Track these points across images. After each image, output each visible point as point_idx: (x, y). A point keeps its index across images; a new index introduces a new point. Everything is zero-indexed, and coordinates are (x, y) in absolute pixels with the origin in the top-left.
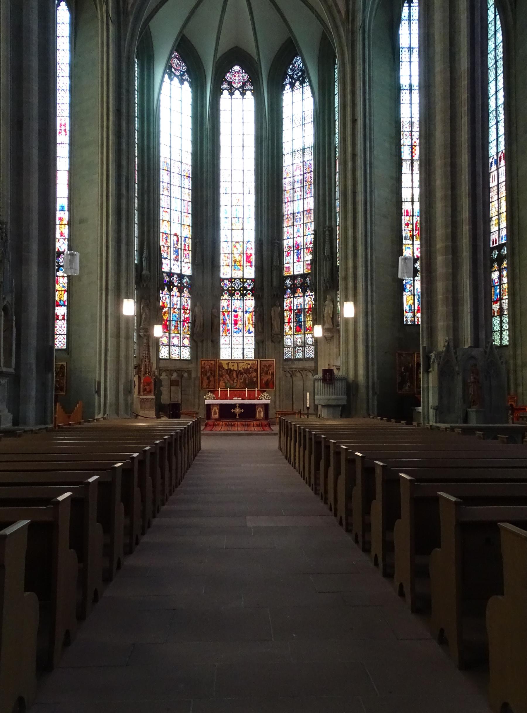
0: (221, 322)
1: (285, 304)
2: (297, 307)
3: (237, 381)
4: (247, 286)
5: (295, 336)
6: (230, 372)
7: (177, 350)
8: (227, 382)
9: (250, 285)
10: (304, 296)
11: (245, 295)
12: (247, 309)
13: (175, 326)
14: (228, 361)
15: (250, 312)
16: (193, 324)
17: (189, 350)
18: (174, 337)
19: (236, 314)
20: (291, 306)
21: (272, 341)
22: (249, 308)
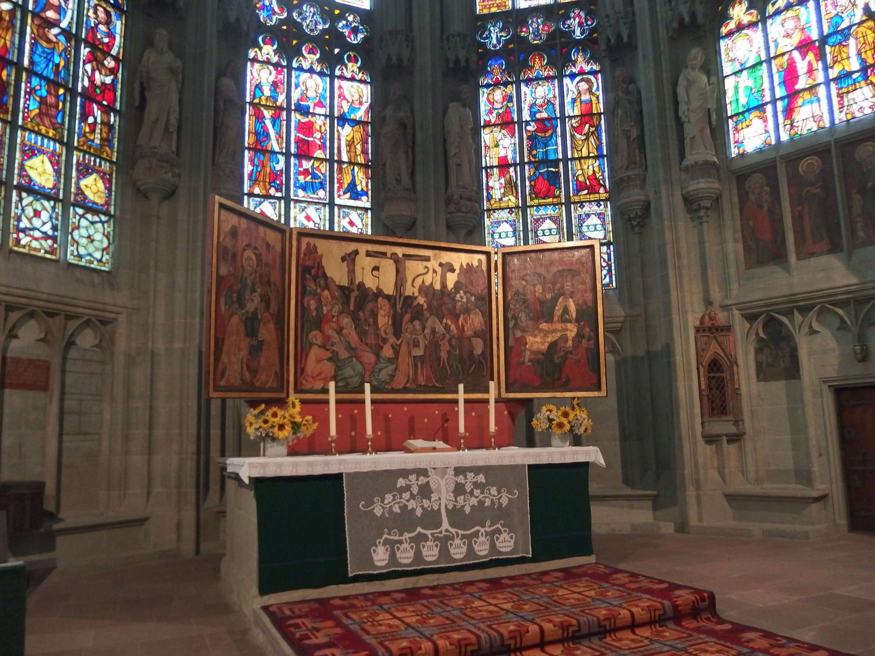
0: (248, 140)
1: (484, 106)
2: (533, 114)
3: (396, 350)
4: (346, 32)
5: (532, 213)
6: (360, 306)
7: (45, 216)
8: (344, 354)
9: (355, 31)
10: (560, 77)
11: (339, 60)
12: (346, 107)
13: (42, 101)
14: (353, 246)
15: (355, 123)
16: (135, 112)
17: (109, 229)
18: (31, 152)
19: (305, 120)
20: (508, 111)
21: (449, 227)
22: (352, 109)
